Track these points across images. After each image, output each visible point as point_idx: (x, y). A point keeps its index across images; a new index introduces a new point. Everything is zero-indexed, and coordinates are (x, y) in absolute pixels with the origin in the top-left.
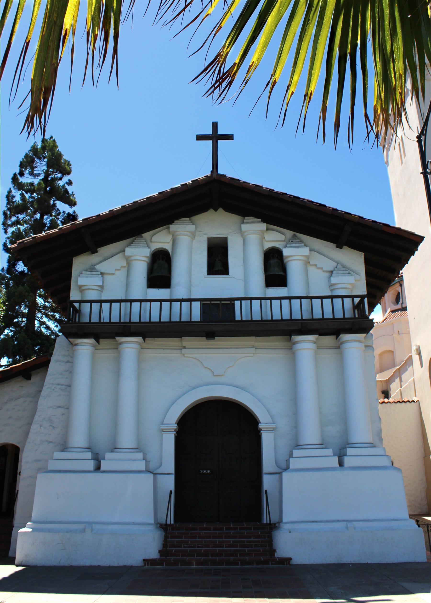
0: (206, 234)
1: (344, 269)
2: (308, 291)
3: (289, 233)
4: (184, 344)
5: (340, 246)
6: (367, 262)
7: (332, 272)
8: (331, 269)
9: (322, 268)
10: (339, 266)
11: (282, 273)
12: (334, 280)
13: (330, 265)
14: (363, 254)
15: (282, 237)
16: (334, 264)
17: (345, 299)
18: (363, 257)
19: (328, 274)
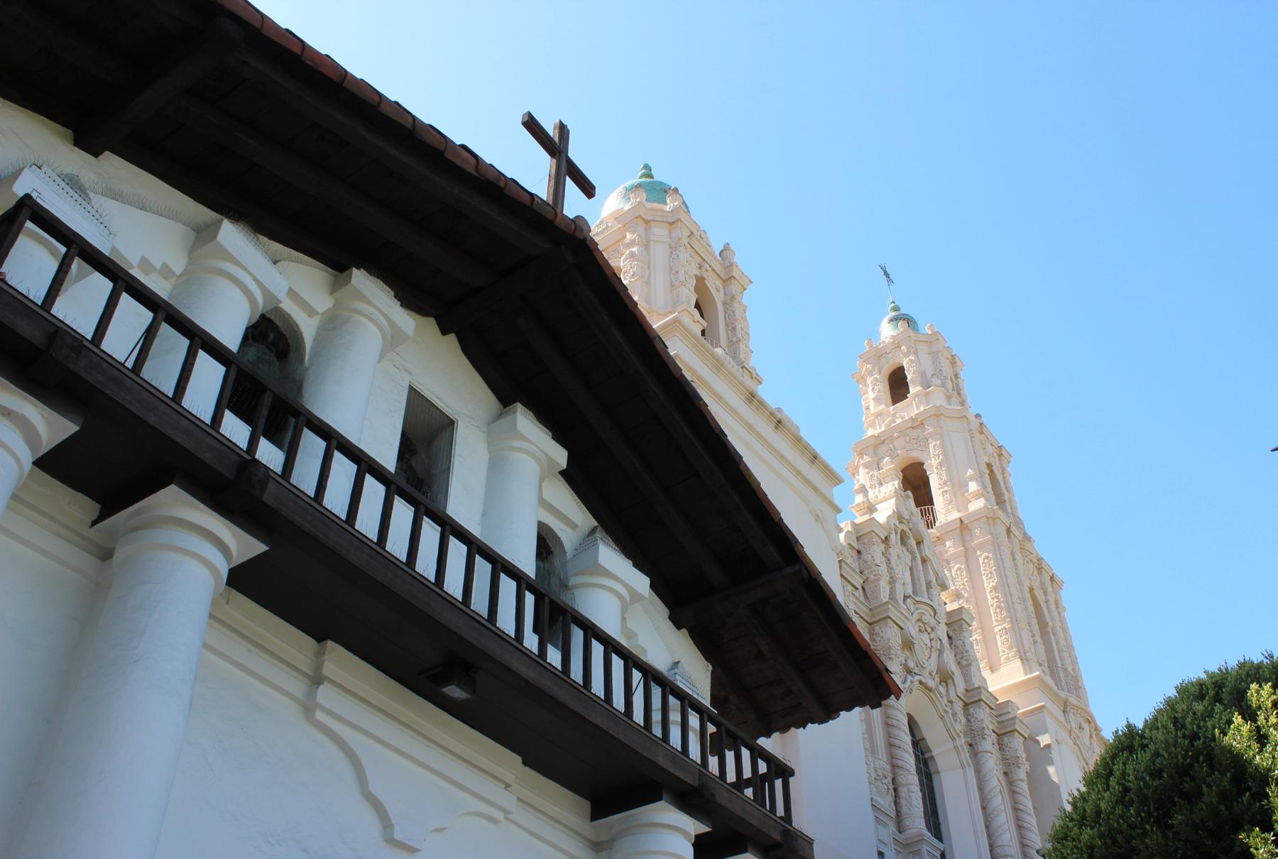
0: (410, 373)
4: (329, 669)
18: (709, 674)
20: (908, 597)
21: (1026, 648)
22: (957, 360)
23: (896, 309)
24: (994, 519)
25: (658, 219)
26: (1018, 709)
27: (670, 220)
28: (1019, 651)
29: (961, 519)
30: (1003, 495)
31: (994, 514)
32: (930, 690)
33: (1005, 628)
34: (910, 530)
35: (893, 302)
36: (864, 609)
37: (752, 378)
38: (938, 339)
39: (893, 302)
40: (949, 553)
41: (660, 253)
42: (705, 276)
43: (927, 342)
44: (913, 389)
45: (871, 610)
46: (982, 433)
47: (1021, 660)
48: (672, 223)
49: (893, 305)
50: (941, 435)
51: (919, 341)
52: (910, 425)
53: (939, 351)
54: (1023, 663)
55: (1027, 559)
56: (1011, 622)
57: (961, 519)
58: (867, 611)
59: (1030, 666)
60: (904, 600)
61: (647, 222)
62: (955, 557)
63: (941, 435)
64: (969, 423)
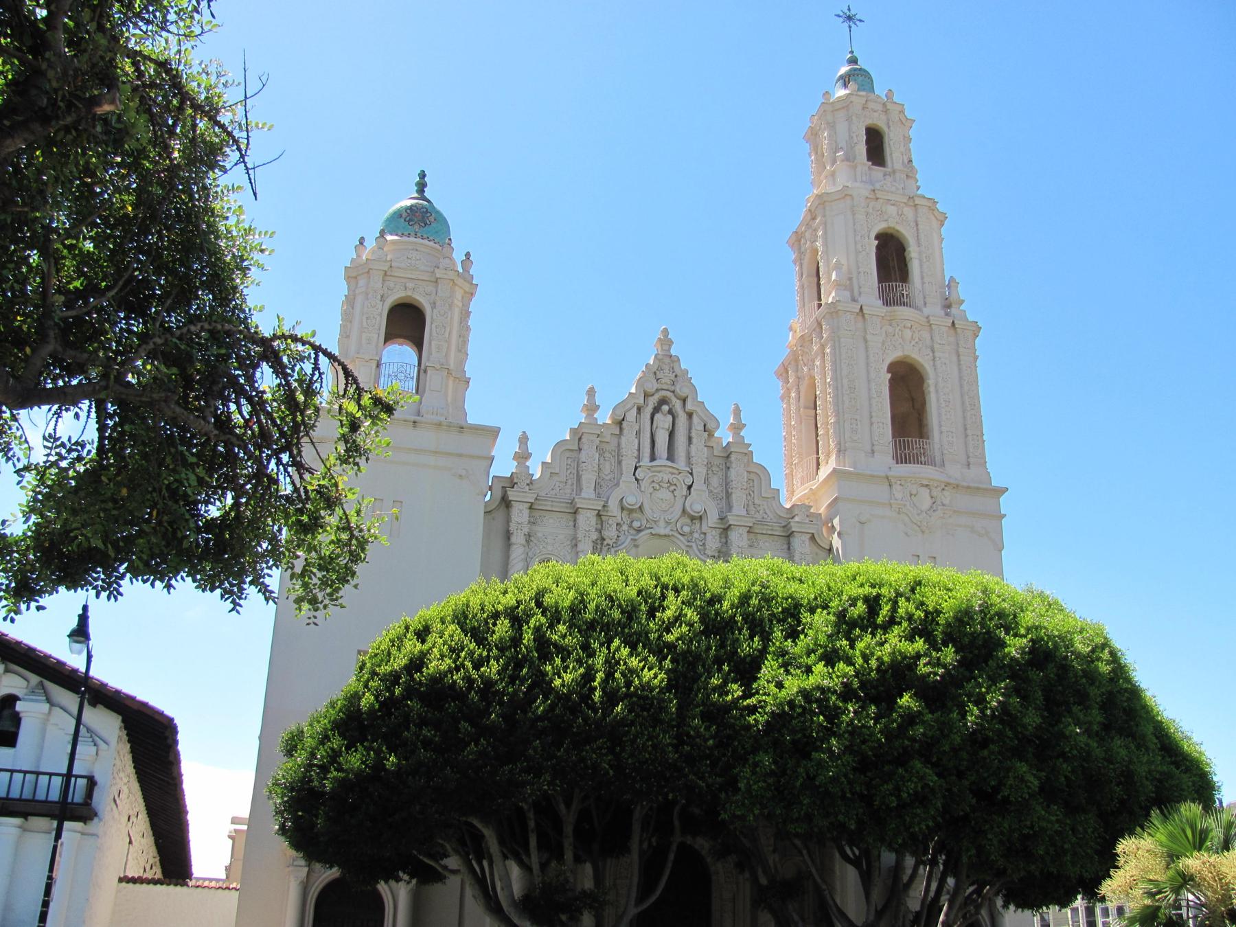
1: (89, 735)
2: (39, 759)
3: (35, 679)
11: (13, 729)
15: (23, 683)
22: (889, 106)
23: (853, 61)
24: (837, 312)
28: (839, 443)
31: (835, 308)
32: (665, 536)
34: (673, 392)
36: (564, 505)
38: (851, 102)
42: (409, 293)
43: (843, 108)
48: (368, 272)
49: (849, 55)
50: (825, 224)
51: (836, 110)
60: (636, 468)
61: (356, 278)
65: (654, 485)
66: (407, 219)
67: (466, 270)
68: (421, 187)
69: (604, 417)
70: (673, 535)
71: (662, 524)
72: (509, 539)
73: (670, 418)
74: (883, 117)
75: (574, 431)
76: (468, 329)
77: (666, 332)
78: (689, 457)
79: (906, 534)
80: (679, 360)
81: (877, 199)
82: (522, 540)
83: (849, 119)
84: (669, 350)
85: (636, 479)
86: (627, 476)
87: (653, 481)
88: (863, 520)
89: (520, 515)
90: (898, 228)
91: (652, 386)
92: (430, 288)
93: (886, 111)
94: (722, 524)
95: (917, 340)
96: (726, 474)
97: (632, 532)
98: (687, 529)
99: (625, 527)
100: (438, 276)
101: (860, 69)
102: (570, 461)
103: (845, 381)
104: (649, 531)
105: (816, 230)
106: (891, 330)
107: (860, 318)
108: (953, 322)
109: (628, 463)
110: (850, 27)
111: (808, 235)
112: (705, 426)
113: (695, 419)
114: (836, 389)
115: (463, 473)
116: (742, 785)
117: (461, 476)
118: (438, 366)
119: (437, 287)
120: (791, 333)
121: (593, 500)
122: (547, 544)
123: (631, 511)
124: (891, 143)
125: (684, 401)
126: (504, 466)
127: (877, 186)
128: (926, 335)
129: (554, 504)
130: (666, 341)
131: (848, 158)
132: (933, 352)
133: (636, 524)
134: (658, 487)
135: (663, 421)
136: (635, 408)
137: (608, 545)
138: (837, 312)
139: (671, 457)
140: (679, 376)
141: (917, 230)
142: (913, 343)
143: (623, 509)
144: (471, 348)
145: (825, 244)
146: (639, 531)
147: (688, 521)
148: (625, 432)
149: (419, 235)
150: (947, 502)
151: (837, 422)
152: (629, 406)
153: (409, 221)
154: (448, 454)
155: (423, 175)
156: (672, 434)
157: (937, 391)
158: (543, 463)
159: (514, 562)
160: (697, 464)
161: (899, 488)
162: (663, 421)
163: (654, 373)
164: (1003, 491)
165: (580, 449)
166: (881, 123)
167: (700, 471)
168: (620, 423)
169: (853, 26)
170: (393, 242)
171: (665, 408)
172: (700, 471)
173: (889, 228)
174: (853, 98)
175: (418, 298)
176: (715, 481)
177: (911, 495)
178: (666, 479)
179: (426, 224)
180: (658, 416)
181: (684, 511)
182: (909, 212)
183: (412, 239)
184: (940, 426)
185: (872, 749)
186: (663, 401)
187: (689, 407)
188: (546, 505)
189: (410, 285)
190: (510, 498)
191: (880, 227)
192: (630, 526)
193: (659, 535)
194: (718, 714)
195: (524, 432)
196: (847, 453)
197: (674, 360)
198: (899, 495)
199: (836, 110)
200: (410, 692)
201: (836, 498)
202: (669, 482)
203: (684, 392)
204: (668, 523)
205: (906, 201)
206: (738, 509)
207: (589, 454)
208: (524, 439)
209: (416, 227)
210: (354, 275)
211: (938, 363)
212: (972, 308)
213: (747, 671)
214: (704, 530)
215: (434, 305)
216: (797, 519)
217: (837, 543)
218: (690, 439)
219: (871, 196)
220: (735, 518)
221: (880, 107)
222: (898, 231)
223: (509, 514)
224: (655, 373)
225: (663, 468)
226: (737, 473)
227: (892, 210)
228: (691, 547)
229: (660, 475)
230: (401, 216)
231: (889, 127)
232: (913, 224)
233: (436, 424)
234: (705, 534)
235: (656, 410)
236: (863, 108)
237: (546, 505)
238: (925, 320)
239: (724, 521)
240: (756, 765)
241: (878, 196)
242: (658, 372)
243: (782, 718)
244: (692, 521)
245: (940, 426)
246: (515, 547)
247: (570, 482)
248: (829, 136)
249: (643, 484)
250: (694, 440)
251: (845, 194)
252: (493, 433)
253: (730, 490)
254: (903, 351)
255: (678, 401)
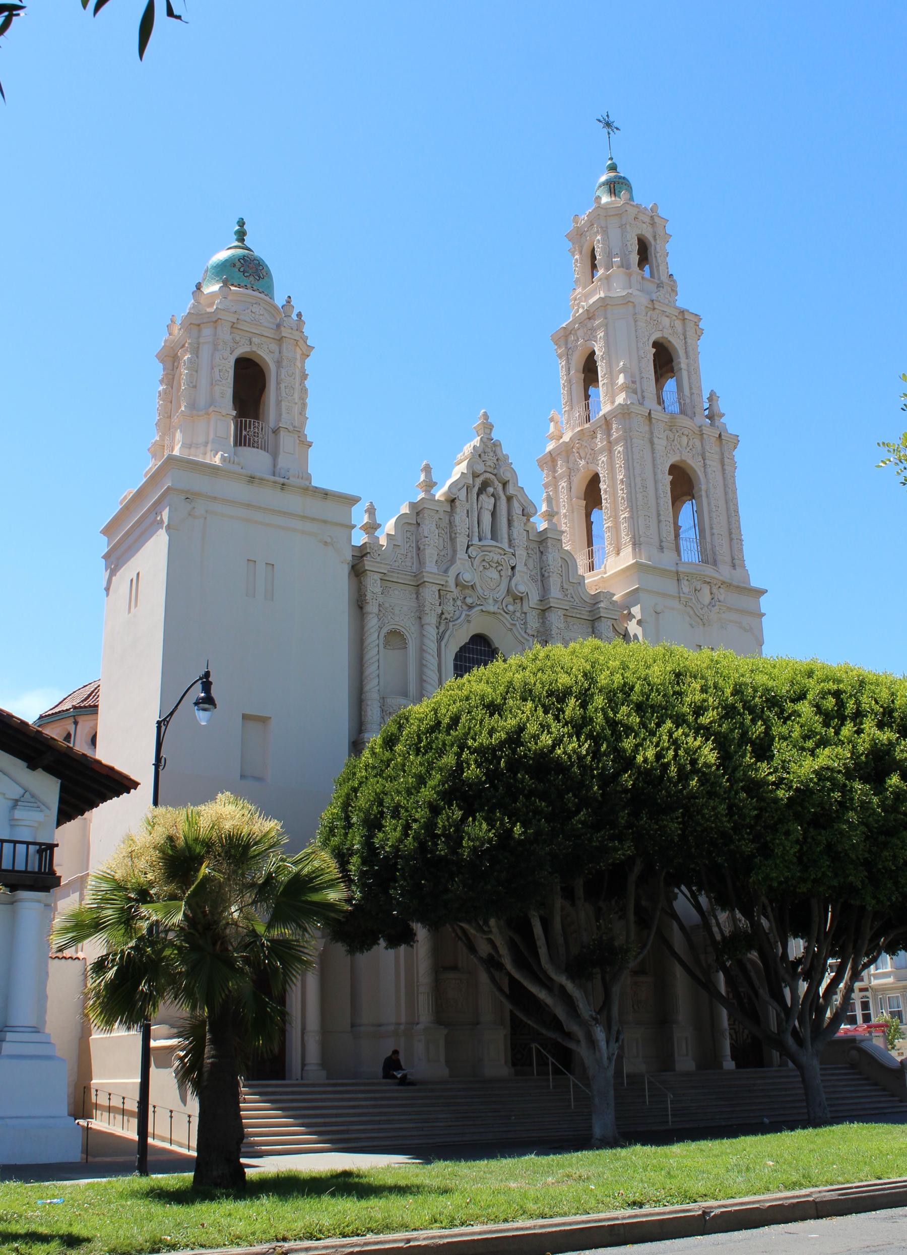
1: (33, 800)
5: (32, 766)
6: (63, 789)
7: (17, 801)
8: (17, 797)
9: (4, 794)
10: (27, 794)
12: (18, 814)
13: (17, 791)
14: (60, 781)
16: (22, 791)
17: (30, 846)
19: (10, 803)
20: (472, 545)
21: (641, 533)
23: (613, 168)
24: (629, 414)
25: (205, 321)
26: (614, 595)
27: (214, 320)
28: (634, 537)
29: (606, 419)
30: (679, 363)
31: (628, 409)
32: (494, 613)
33: (625, 517)
34: (495, 475)
35: (611, 159)
36: (409, 577)
37: (289, 432)
39: (611, 159)
40: (599, 447)
41: (205, 351)
42: (254, 349)
44: (601, 272)
45: (415, 576)
46: (654, 309)
47: (634, 544)
48: (216, 322)
49: (609, 162)
50: (606, 325)
51: (609, 216)
52: (586, 316)
53: (626, 224)
54: (634, 549)
55: (678, 434)
56: (631, 511)
57: (606, 419)
58: (412, 578)
59: (640, 550)
60: (468, 547)
61: (199, 325)
62: (601, 451)
63: (606, 325)
64: (634, 306)
65: (484, 563)
66: (242, 269)
67: (299, 329)
68: (241, 235)
69: (440, 493)
70: (500, 614)
71: (491, 601)
72: (361, 608)
73: (493, 499)
74: (650, 229)
75: (413, 505)
76: (306, 390)
77: (486, 416)
78: (510, 541)
79: (691, 625)
80: (500, 444)
81: (654, 309)
82: (376, 610)
83: (622, 227)
84: (490, 434)
85: (470, 557)
86: (461, 554)
87: (484, 560)
88: (659, 610)
89: (373, 585)
90: (671, 339)
91: (480, 468)
92: (274, 347)
93: (653, 224)
94: (541, 605)
95: (691, 447)
96: (541, 558)
97: (465, 607)
98: (511, 608)
99: (459, 603)
100: (283, 334)
101: (620, 178)
102: (409, 534)
103: (638, 480)
104: (481, 607)
105: (593, 330)
106: (671, 435)
107: (647, 422)
108: (720, 435)
109: (461, 541)
110: (609, 133)
111: (580, 333)
112: (523, 510)
113: (516, 504)
114: (629, 486)
115: (329, 540)
116: (778, 851)
117: (326, 542)
118: (291, 428)
119: (280, 346)
120: (552, 424)
121: (435, 574)
122: (394, 614)
123: (464, 587)
124: (658, 255)
125: (505, 484)
126: (359, 538)
127: (654, 297)
128: (698, 443)
129: (400, 576)
130: (487, 427)
131: (625, 265)
132: (704, 459)
133: (469, 601)
134: (488, 566)
135: (488, 502)
136: (465, 487)
137: (446, 619)
138: (629, 414)
139: (494, 537)
140: (500, 461)
141: (686, 343)
142: (688, 449)
143: (457, 585)
144: (308, 413)
145: (607, 345)
146: (470, 607)
147: (511, 600)
148: (458, 510)
149: (255, 288)
150: (721, 599)
151: (631, 517)
152: (460, 486)
153: (244, 272)
154: (314, 519)
155: (241, 223)
156: (494, 514)
157: (707, 496)
158: (388, 535)
159: (372, 631)
160: (518, 547)
161: (686, 583)
162: (488, 502)
163: (479, 455)
164: (763, 592)
165: (418, 524)
166: (649, 235)
167: (521, 552)
168: (452, 502)
169: (611, 132)
170: (236, 293)
171: (490, 490)
172: (521, 552)
173: (663, 337)
174: (628, 208)
175: (262, 354)
176: (531, 564)
177: (696, 590)
178: (495, 560)
179: (260, 277)
180: (483, 497)
181: (509, 591)
182: (678, 324)
183: (250, 292)
184: (712, 528)
185: (877, 821)
186: (485, 485)
187: (511, 490)
188: (392, 576)
189: (255, 340)
190: (367, 568)
191: (656, 336)
192: (464, 602)
193: (489, 612)
194: (755, 787)
195: (371, 503)
196: (642, 546)
197: (497, 445)
198: (686, 590)
199: (609, 216)
200: (515, 765)
201: (637, 589)
202: (498, 562)
203: (507, 476)
204: (496, 601)
205: (677, 314)
206: (555, 592)
207: (429, 528)
208: (371, 511)
209: (251, 278)
210: (198, 322)
211: (709, 470)
212: (731, 423)
213: (763, 751)
214: (525, 610)
215: (279, 363)
216: (602, 605)
217: (633, 628)
218: (510, 523)
219: (649, 306)
220: (556, 601)
221: (647, 220)
222: (669, 342)
223: (361, 583)
224: (480, 456)
225: (493, 549)
226: (552, 558)
227: (666, 321)
228: (515, 625)
229: (491, 554)
230: (234, 265)
231: (655, 240)
232: (682, 337)
233: (303, 489)
234: (525, 613)
235: (481, 491)
236: (636, 218)
237: (392, 576)
238: (698, 429)
239: (543, 603)
240: (787, 833)
241: (656, 307)
242: (483, 455)
243: (803, 794)
244: (514, 600)
245: (712, 528)
246: (371, 616)
247: (409, 554)
248: (603, 239)
249: (477, 562)
250: (516, 524)
251: (626, 301)
252: (353, 500)
253: (546, 575)
254: (681, 456)
255: (500, 484)
